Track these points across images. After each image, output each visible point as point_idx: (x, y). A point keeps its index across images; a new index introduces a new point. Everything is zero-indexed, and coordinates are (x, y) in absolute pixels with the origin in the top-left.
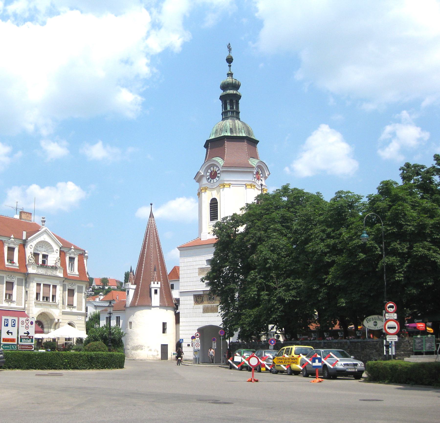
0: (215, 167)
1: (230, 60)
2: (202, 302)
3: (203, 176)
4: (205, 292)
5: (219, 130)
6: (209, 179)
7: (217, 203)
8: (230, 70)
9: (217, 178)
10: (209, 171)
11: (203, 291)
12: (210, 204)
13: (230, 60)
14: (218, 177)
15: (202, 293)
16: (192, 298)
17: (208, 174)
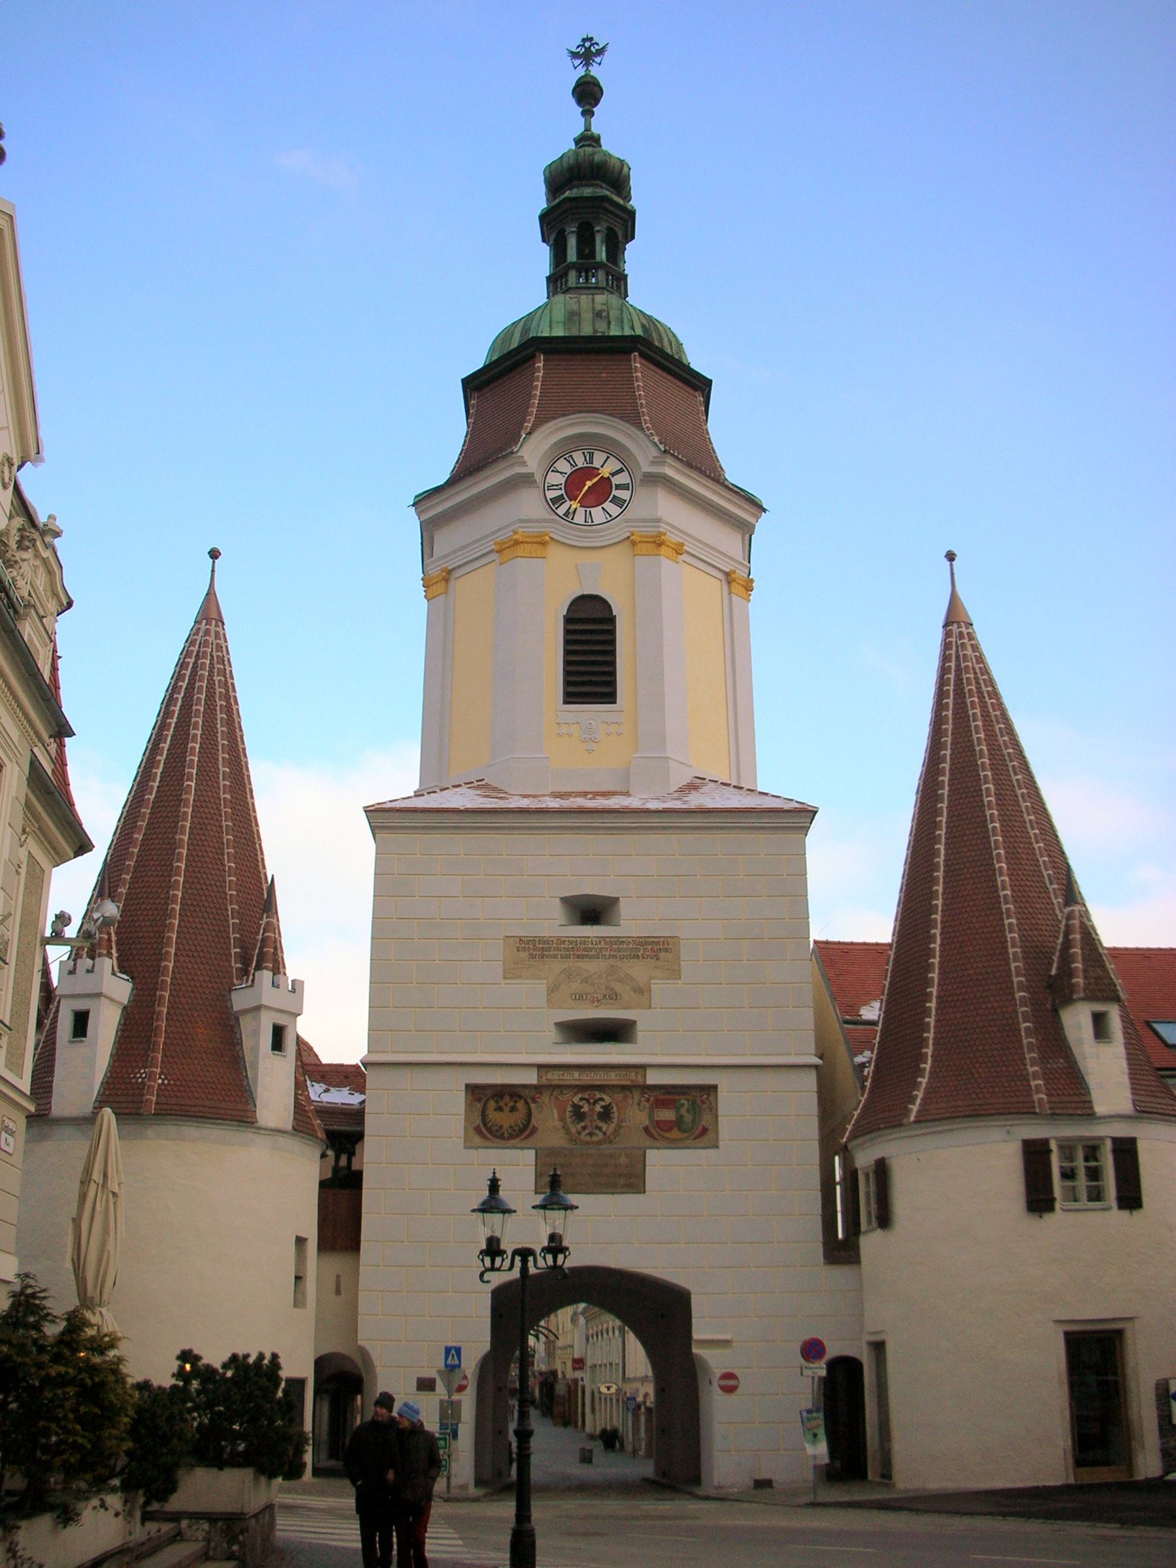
0: (598, 459)
1: (588, 94)
2: (523, 1132)
3: (526, 480)
4: (554, 1077)
5: (587, 316)
6: (558, 501)
7: (612, 620)
8: (588, 129)
9: (608, 505)
10: (564, 467)
11: (540, 1067)
12: (568, 620)
13: (588, 94)
14: (617, 501)
15: (531, 1078)
16: (458, 1102)
17: (557, 479)
